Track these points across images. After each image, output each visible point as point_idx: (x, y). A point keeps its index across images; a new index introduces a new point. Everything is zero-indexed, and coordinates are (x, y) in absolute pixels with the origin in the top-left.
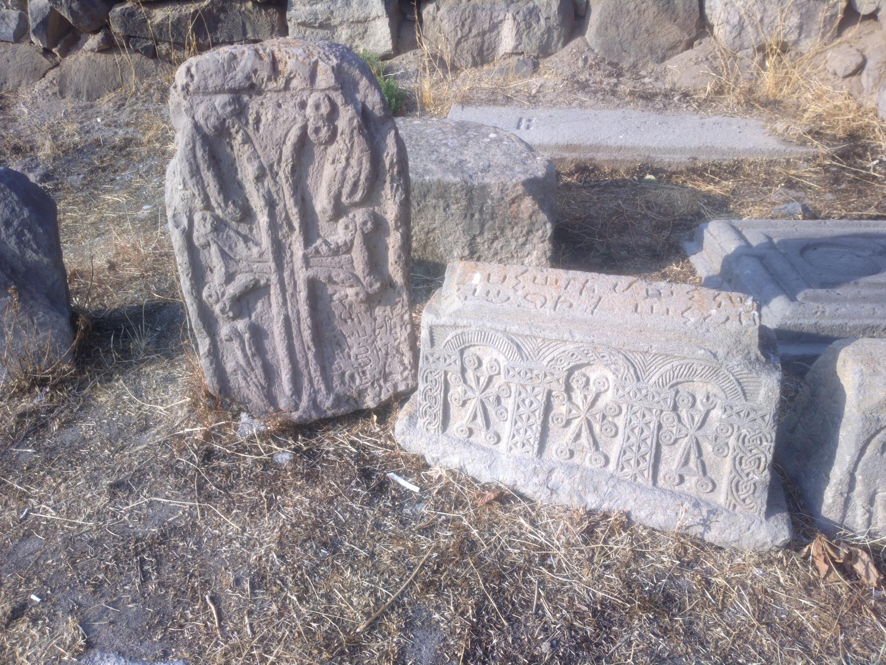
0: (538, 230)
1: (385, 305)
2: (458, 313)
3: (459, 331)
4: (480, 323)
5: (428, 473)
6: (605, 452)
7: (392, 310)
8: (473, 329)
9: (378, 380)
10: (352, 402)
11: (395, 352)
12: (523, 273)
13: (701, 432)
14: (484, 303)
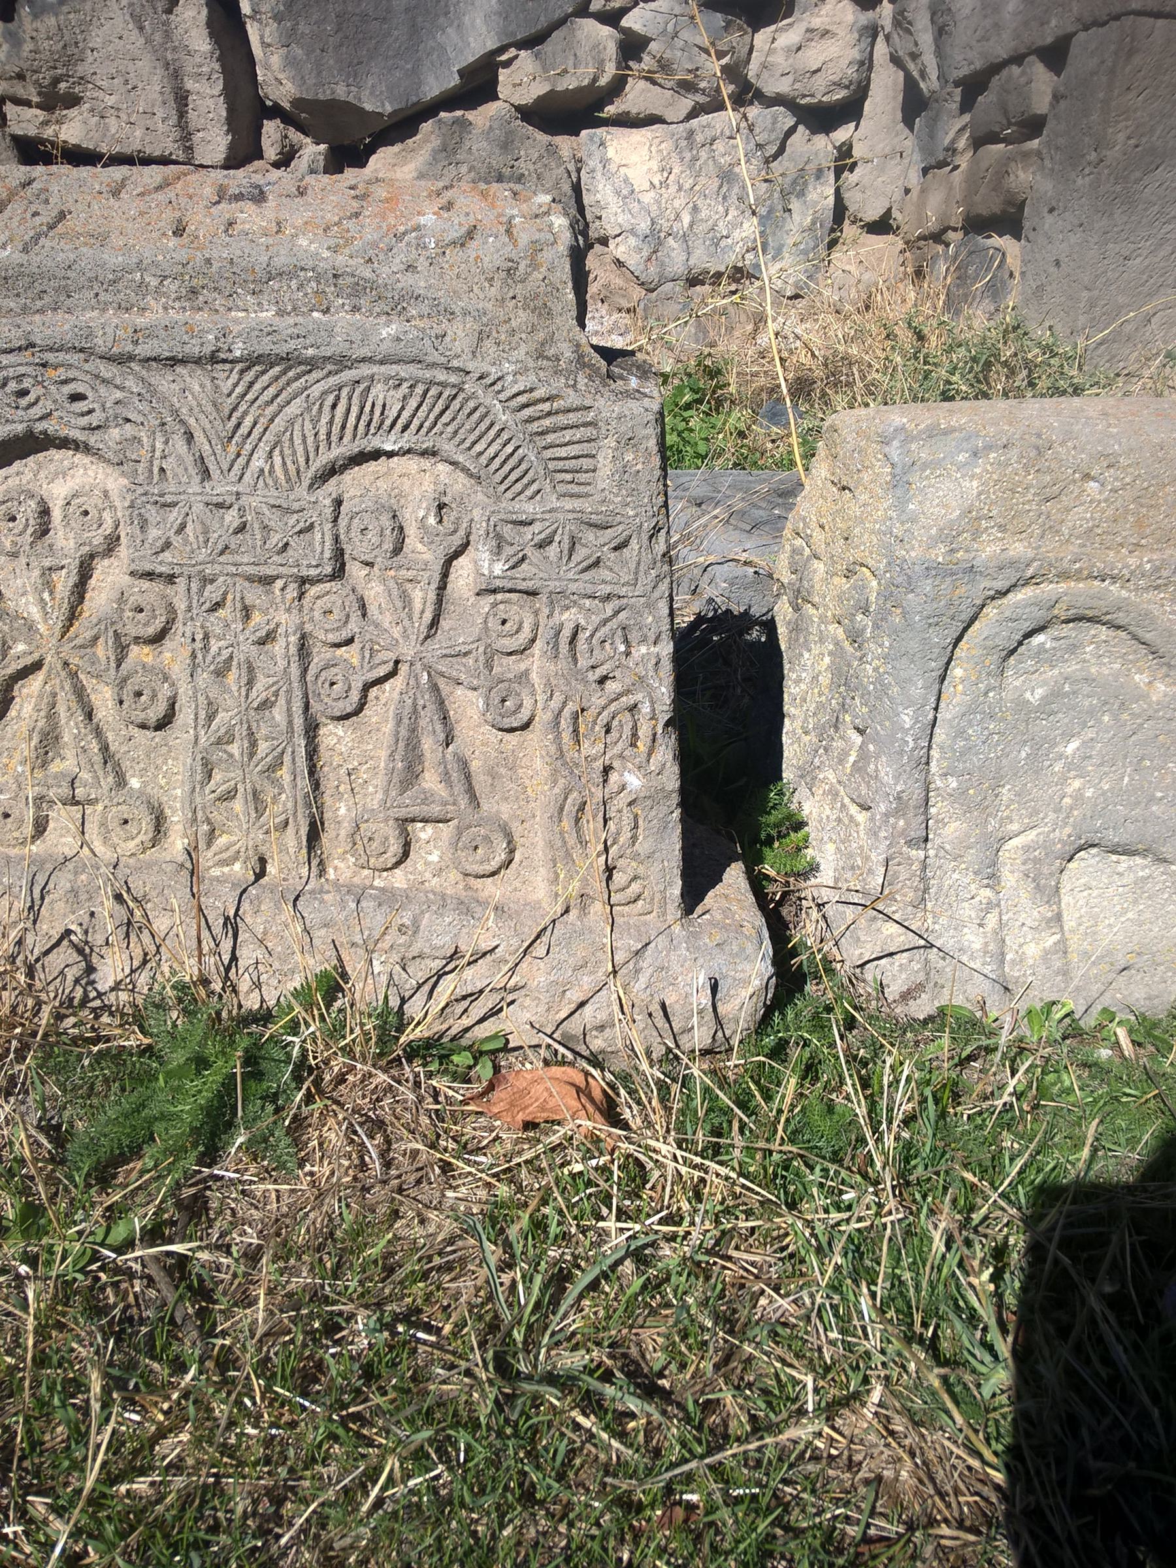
6: (154, 792)
13: (437, 645)
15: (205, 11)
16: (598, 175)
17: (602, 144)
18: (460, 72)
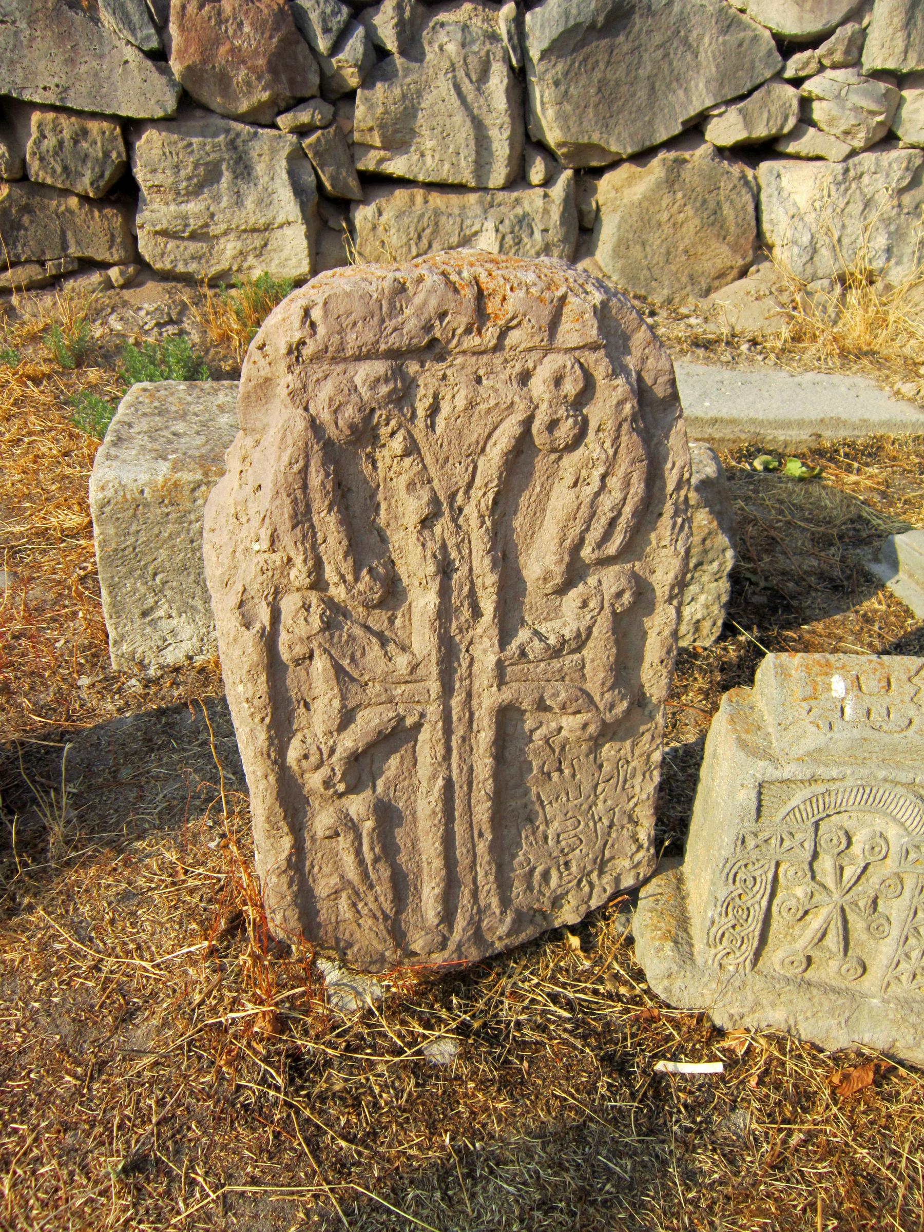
0: (711, 562)
1: (623, 739)
2: (816, 755)
3: (819, 788)
4: (864, 772)
5: (725, 1044)
7: (634, 745)
8: (849, 782)
9: (589, 874)
10: (539, 918)
11: (625, 821)
12: (917, 673)
14: (869, 734)
15: (506, 81)
16: (774, 199)
17: (779, 176)
18: (683, 123)
